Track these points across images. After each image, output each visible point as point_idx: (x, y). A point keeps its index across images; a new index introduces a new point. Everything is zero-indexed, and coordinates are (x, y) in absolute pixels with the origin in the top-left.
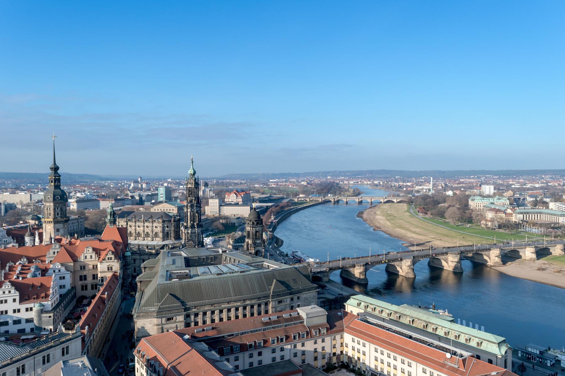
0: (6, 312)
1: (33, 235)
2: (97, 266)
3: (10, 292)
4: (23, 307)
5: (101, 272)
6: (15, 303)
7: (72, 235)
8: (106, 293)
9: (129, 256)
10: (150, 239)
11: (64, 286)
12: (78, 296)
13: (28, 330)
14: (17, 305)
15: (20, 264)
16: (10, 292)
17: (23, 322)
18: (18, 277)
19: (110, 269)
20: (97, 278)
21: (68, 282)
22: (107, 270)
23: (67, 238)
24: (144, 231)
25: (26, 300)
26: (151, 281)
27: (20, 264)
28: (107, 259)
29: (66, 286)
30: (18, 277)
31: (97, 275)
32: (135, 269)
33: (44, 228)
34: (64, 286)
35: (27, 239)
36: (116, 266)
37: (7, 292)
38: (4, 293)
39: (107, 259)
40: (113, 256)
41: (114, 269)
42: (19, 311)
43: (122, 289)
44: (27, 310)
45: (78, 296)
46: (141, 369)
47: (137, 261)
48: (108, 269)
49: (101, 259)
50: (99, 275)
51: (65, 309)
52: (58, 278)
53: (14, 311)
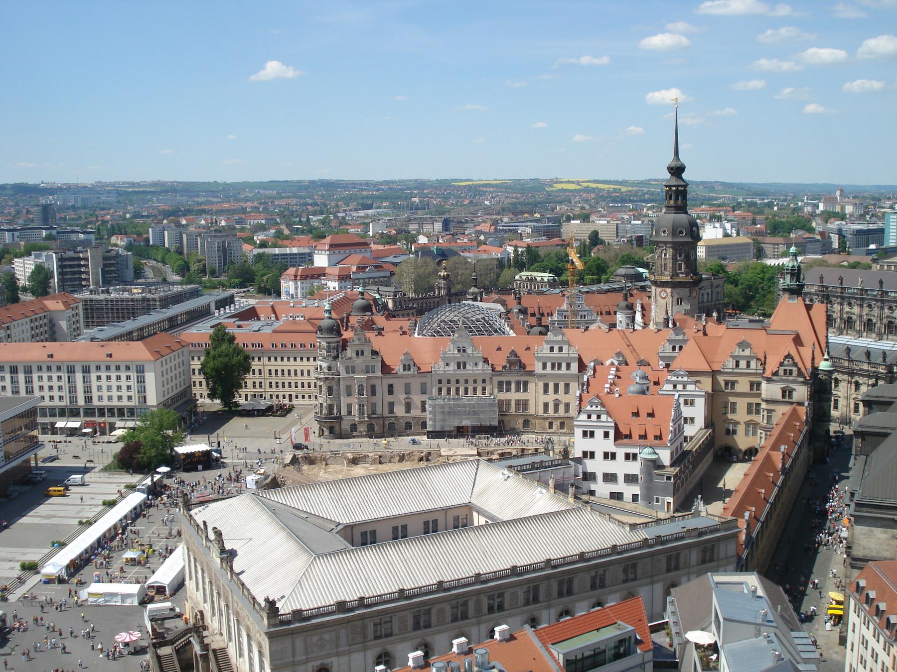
0: (592, 455)
1: (631, 307)
2: (759, 384)
3: (599, 417)
4: (621, 452)
5: (767, 401)
6: (606, 440)
7: (709, 315)
8: (783, 448)
9: (830, 373)
10: (874, 335)
11: (692, 420)
12: (717, 446)
13: (628, 496)
14: (609, 445)
15: (612, 364)
16: (599, 417)
17: (621, 478)
18: (611, 392)
19: (787, 393)
20: (758, 412)
21: (698, 411)
22: (778, 396)
23: (699, 318)
24: (861, 316)
25: (626, 437)
26: (886, 435)
27: (612, 364)
28: (781, 372)
29: (696, 421)
30: (611, 392)
31: (758, 405)
32: (836, 402)
33: (653, 295)
34: (692, 420)
35: (620, 317)
36: (801, 392)
37: (594, 417)
38: (589, 417)
39: (781, 372)
40: (794, 369)
41: (796, 397)
42: (613, 456)
43: (810, 443)
44: (627, 457)
45: (717, 446)
46: (864, 628)
47: (843, 386)
48: (784, 396)
49: (768, 374)
50: (764, 405)
51: (694, 467)
52: (682, 400)
53: (606, 455)
